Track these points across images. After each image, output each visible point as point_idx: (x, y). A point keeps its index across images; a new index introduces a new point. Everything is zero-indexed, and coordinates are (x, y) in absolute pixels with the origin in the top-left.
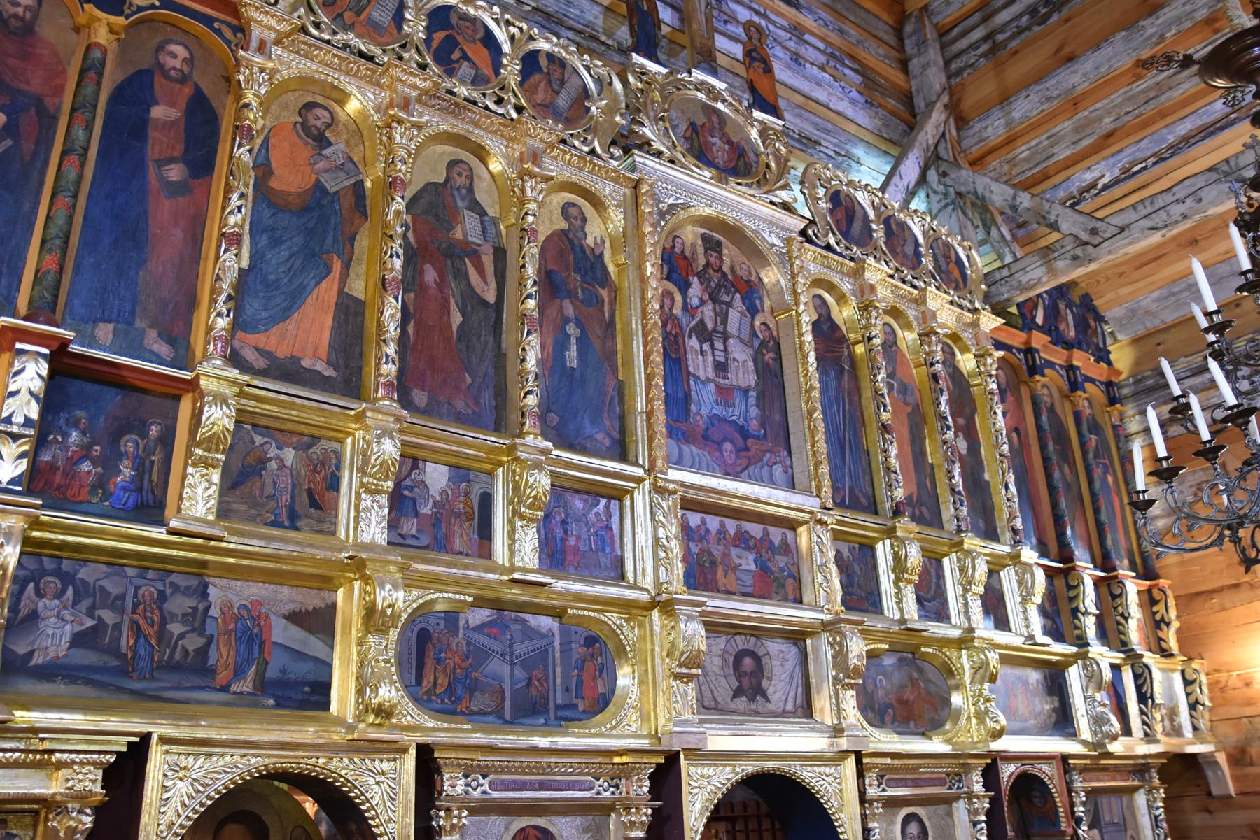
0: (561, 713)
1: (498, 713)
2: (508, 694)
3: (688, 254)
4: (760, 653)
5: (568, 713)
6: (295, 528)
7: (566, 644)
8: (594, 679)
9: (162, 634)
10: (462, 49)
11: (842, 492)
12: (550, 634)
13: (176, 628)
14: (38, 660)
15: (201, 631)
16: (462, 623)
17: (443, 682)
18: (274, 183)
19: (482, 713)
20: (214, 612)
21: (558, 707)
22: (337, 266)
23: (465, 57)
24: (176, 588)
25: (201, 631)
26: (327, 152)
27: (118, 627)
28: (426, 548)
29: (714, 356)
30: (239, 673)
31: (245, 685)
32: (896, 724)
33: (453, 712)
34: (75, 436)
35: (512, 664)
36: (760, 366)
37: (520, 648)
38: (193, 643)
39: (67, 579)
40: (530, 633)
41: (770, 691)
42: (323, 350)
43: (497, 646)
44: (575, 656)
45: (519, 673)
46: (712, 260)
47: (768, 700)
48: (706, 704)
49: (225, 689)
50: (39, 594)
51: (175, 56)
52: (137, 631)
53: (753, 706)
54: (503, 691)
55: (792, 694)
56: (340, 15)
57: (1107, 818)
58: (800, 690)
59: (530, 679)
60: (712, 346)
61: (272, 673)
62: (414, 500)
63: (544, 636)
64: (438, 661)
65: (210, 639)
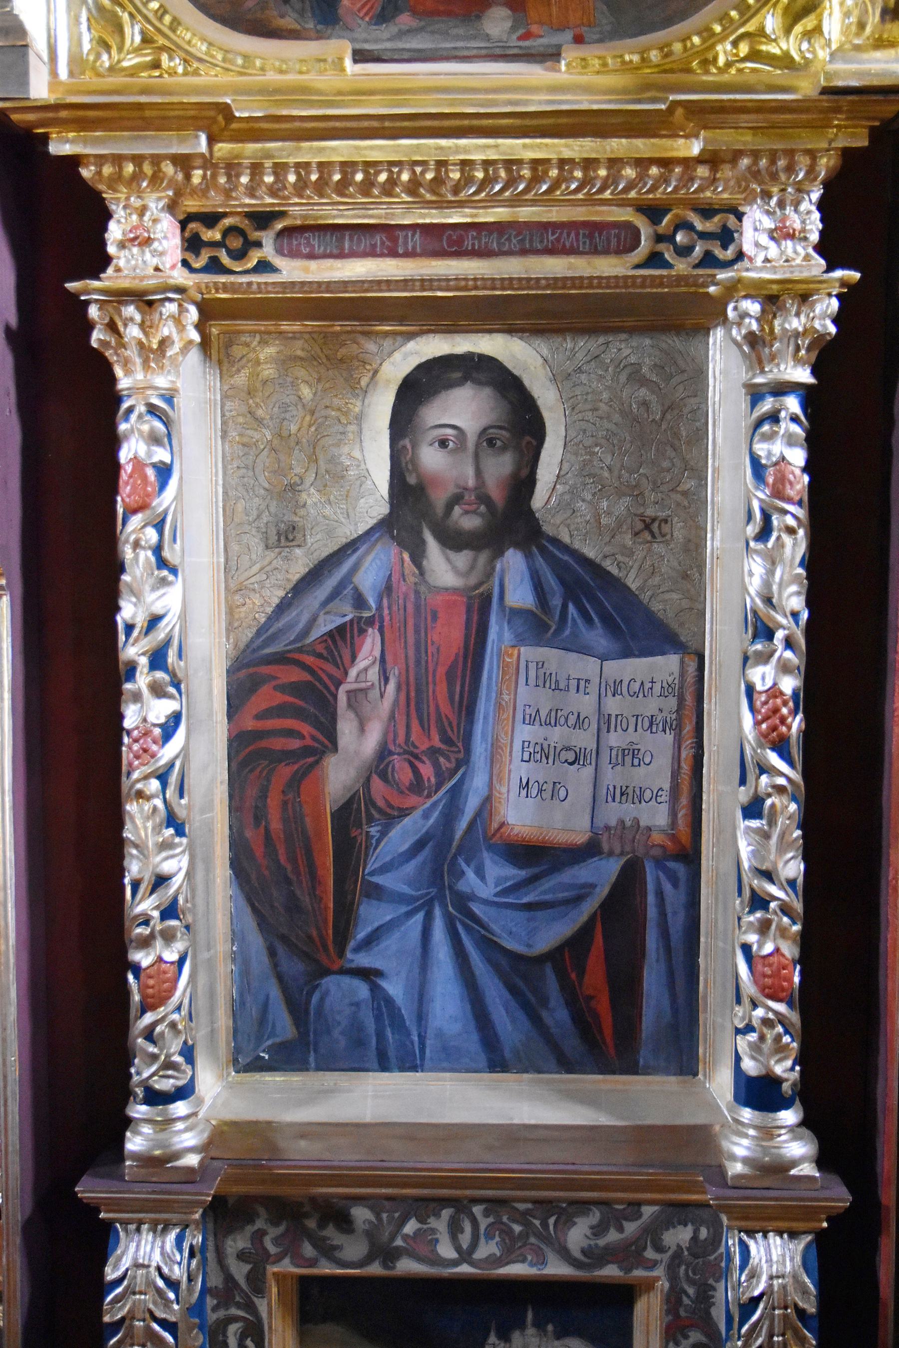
32: (405, 20)
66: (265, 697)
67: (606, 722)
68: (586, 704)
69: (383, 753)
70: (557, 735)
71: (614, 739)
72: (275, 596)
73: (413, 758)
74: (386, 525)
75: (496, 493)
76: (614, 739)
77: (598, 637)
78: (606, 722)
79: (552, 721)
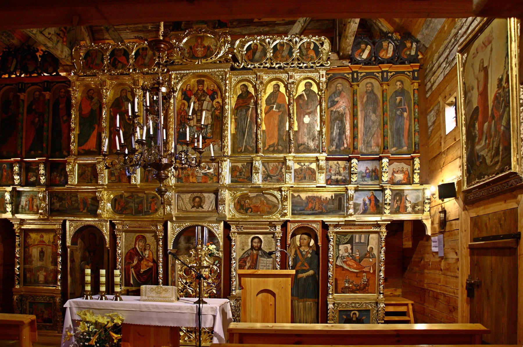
0: (146, 213)
1: (132, 214)
2: (134, 210)
3: (191, 89)
4: (201, 197)
5: (147, 213)
6: (91, 183)
7: (147, 200)
8: (154, 206)
9: (71, 204)
10: (118, 60)
11: (241, 148)
12: (143, 197)
13: (73, 203)
14: (55, 209)
15: (77, 203)
16: (123, 196)
17: (120, 208)
18: (83, 113)
19: (128, 214)
20: (79, 199)
21: (145, 212)
22: (97, 127)
23: (119, 62)
24: (73, 196)
25: (77, 203)
26: (93, 101)
27: (65, 203)
28: (117, 182)
29: (197, 117)
30: (84, 209)
31: (85, 211)
33: (122, 214)
34: (55, 173)
35: (134, 204)
36: (214, 116)
37: (136, 200)
38: (76, 205)
39: (57, 196)
40: (138, 197)
41: (204, 206)
42: (95, 147)
43: (131, 201)
44: (149, 201)
45: (136, 205)
46: (200, 88)
47: (203, 208)
48: (183, 209)
49: (82, 212)
50: (54, 199)
51: (62, 92)
52: (68, 204)
53: (198, 210)
54: (132, 209)
55: (211, 206)
56: (89, 66)
57: (357, 241)
58: (214, 205)
59: (138, 207)
60: (197, 116)
61: (89, 209)
62: (114, 173)
63: (142, 197)
64: (119, 204)
65: (79, 204)
66: (241, 261)
67: (267, 263)
68: (265, 262)
69: (250, 266)
70: (263, 264)
71: (267, 265)
72: (242, 254)
73: (252, 266)
74: (250, 249)
75: (259, 246)
76: (267, 265)
77: (266, 257)
78: (267, 263)
79: (263, 263)
